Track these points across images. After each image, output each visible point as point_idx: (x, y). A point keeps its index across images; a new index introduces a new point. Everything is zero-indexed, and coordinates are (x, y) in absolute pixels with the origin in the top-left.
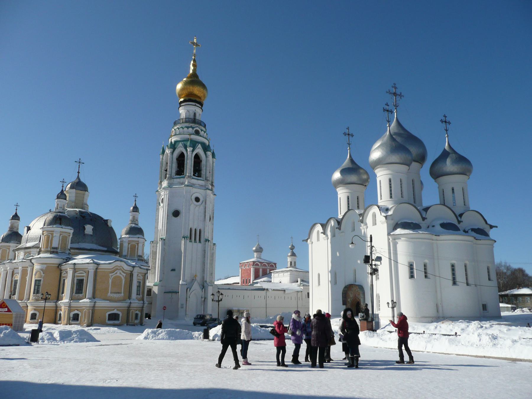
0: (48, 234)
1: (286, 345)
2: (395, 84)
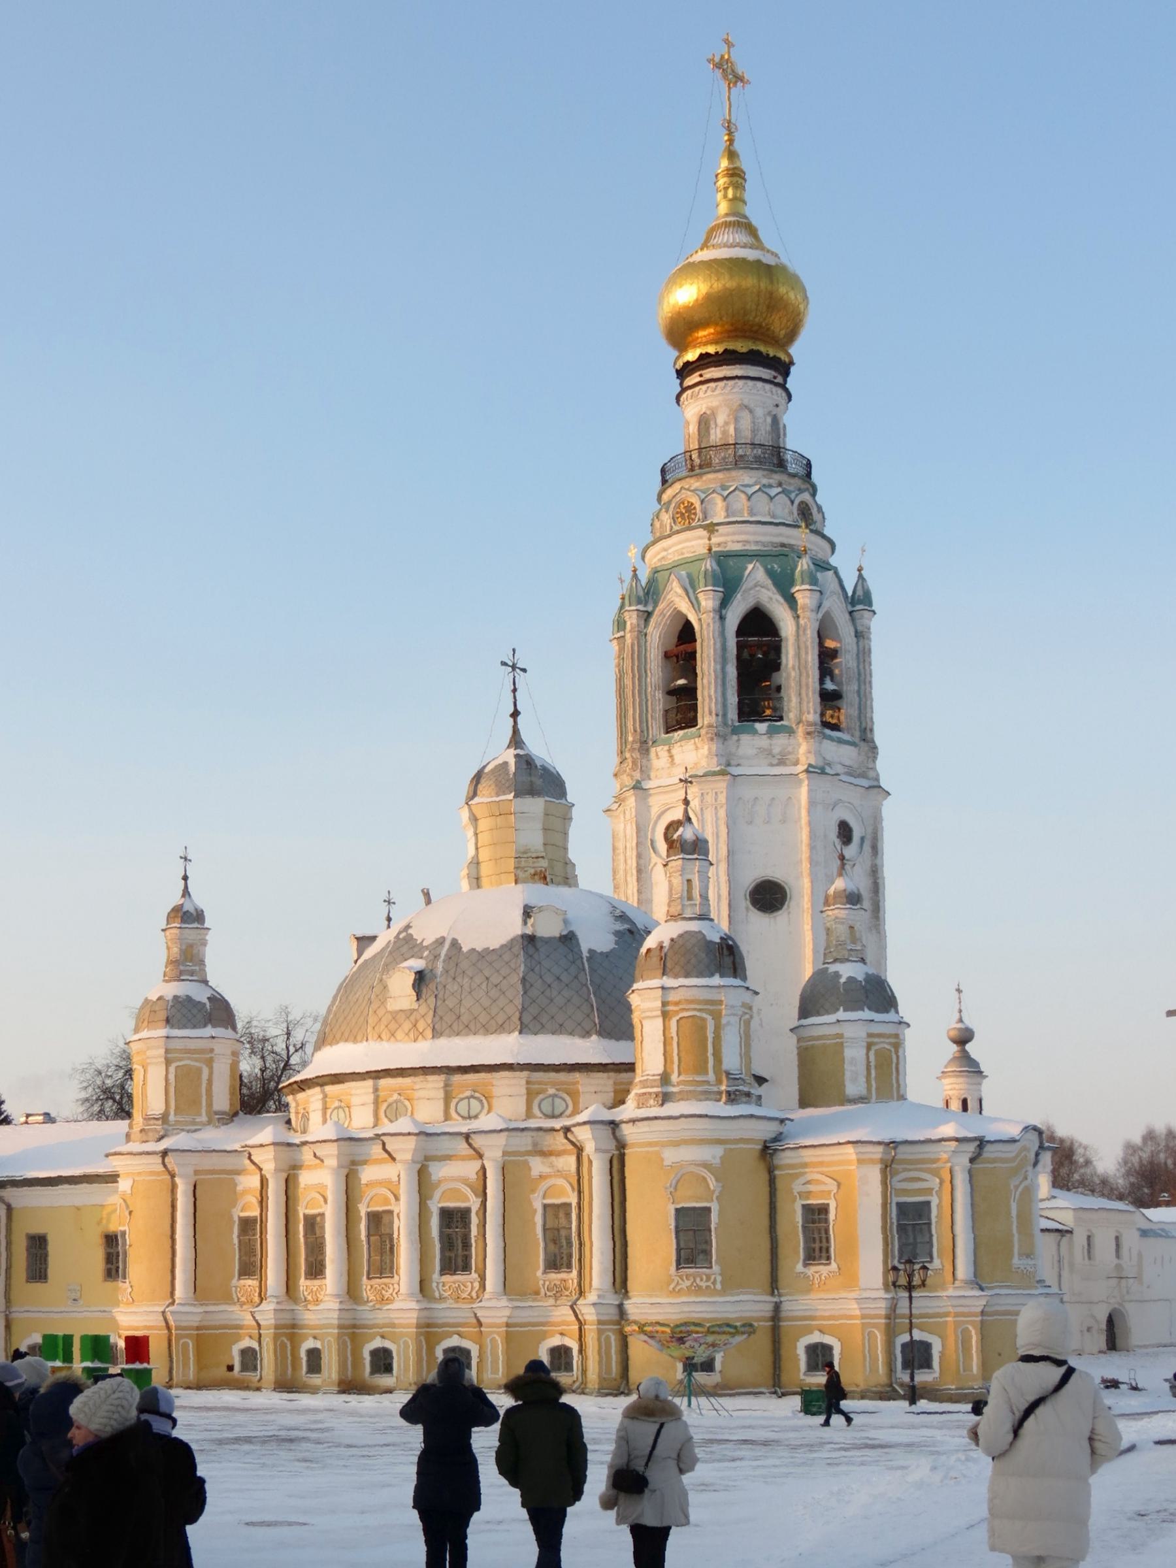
0: (698, 1014)
1: (476, 1505)
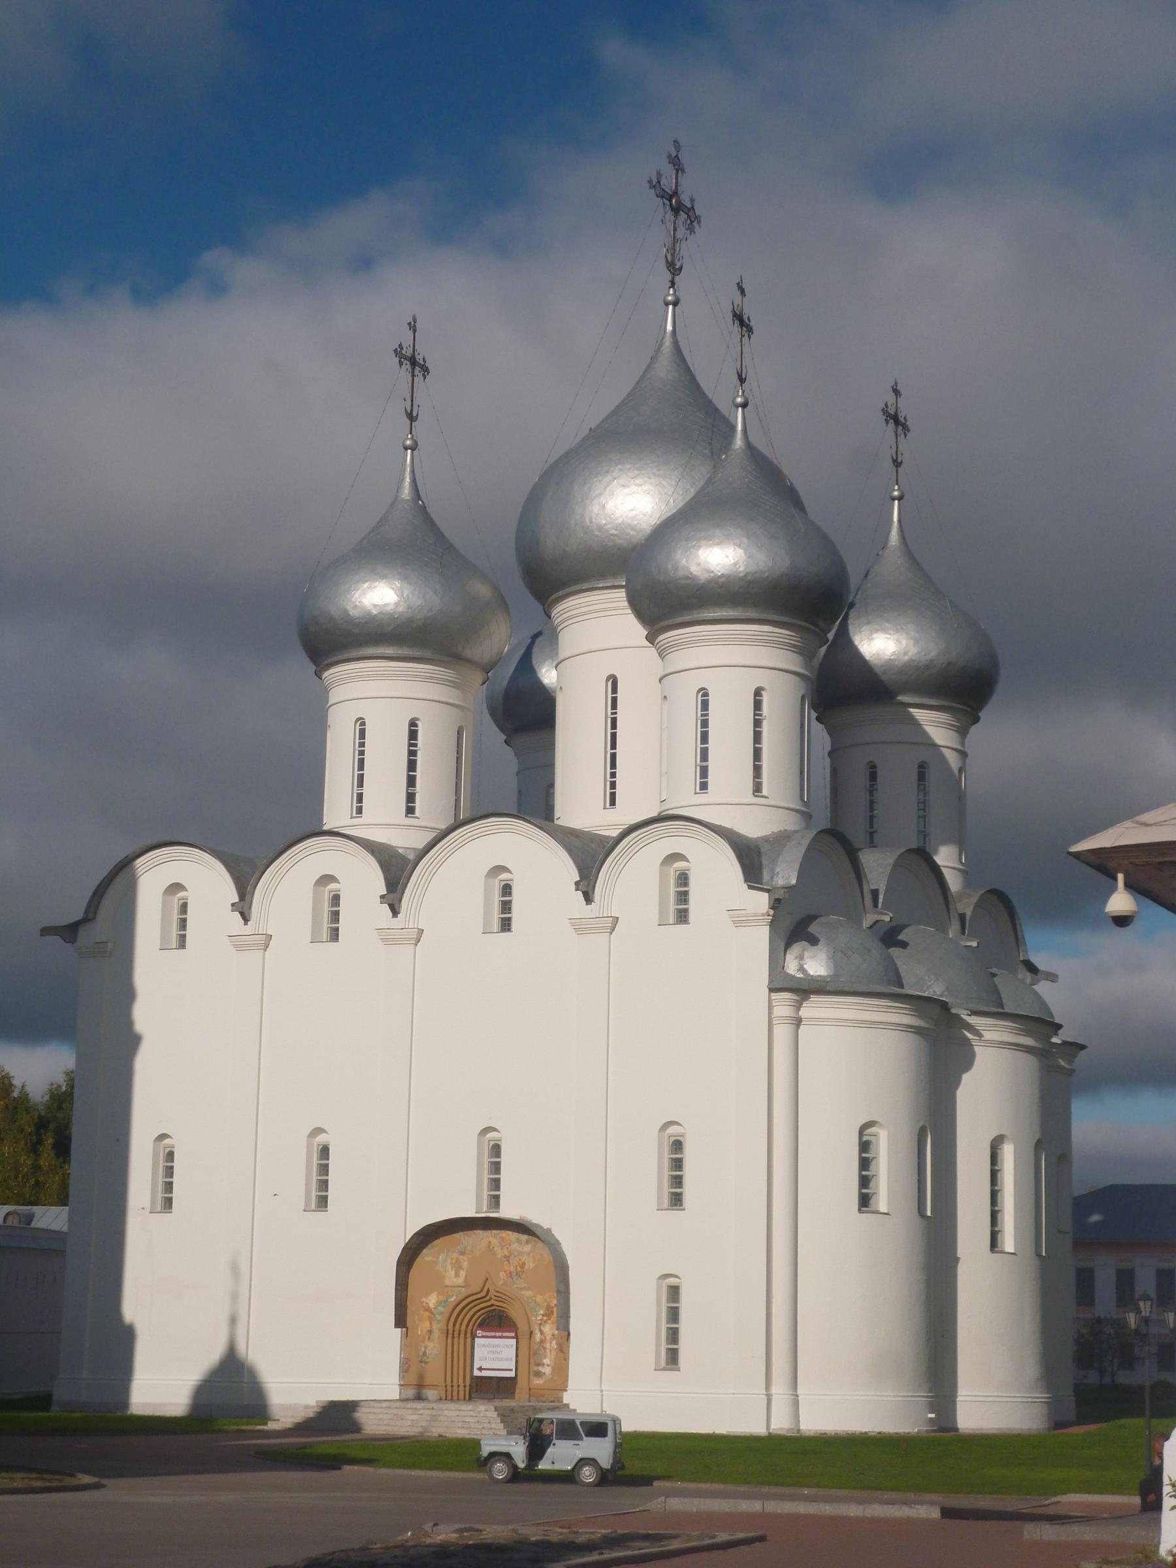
2: (677, 144)
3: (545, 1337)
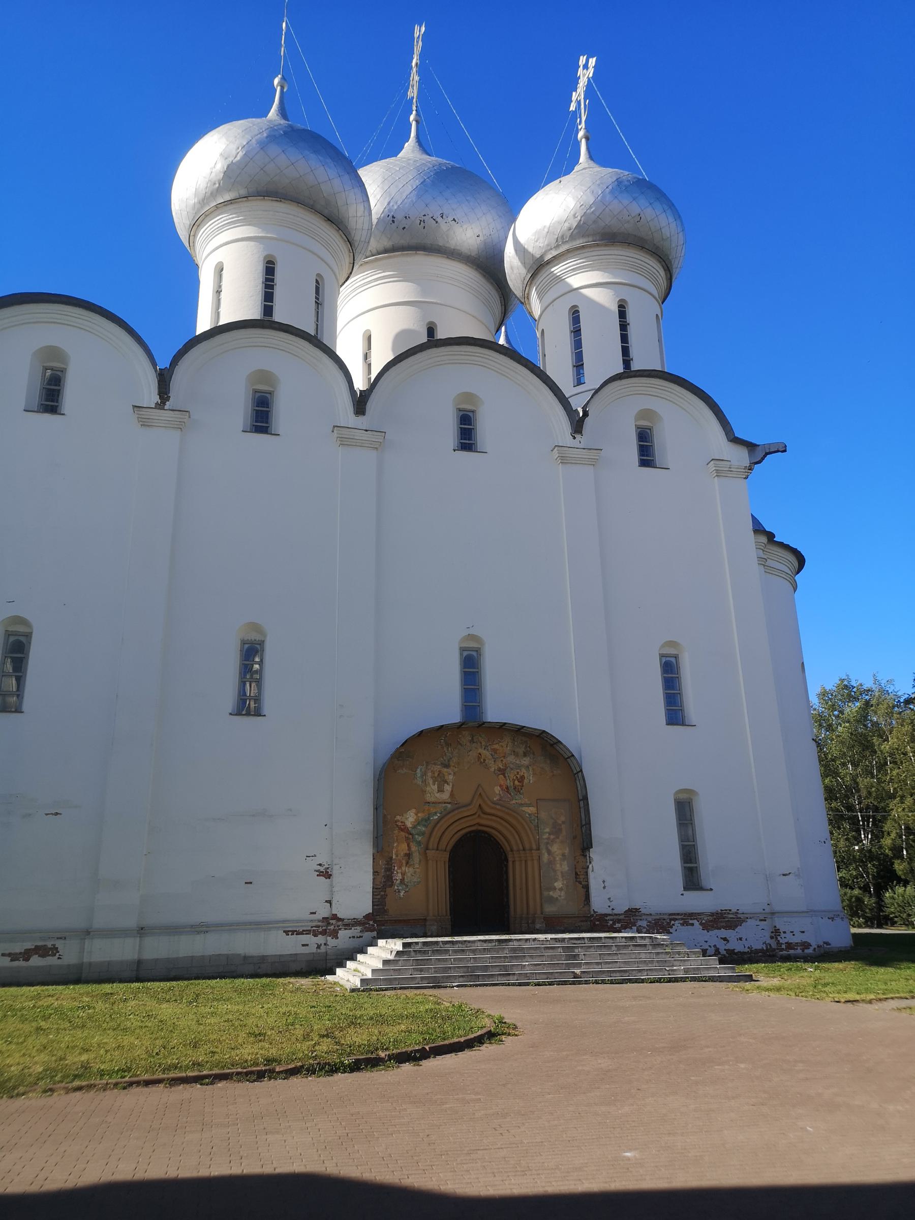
3: (554, 858)
